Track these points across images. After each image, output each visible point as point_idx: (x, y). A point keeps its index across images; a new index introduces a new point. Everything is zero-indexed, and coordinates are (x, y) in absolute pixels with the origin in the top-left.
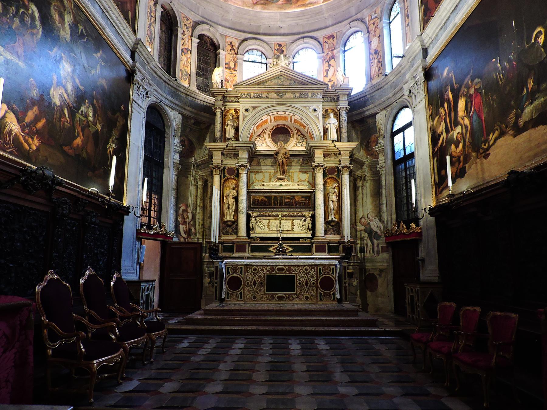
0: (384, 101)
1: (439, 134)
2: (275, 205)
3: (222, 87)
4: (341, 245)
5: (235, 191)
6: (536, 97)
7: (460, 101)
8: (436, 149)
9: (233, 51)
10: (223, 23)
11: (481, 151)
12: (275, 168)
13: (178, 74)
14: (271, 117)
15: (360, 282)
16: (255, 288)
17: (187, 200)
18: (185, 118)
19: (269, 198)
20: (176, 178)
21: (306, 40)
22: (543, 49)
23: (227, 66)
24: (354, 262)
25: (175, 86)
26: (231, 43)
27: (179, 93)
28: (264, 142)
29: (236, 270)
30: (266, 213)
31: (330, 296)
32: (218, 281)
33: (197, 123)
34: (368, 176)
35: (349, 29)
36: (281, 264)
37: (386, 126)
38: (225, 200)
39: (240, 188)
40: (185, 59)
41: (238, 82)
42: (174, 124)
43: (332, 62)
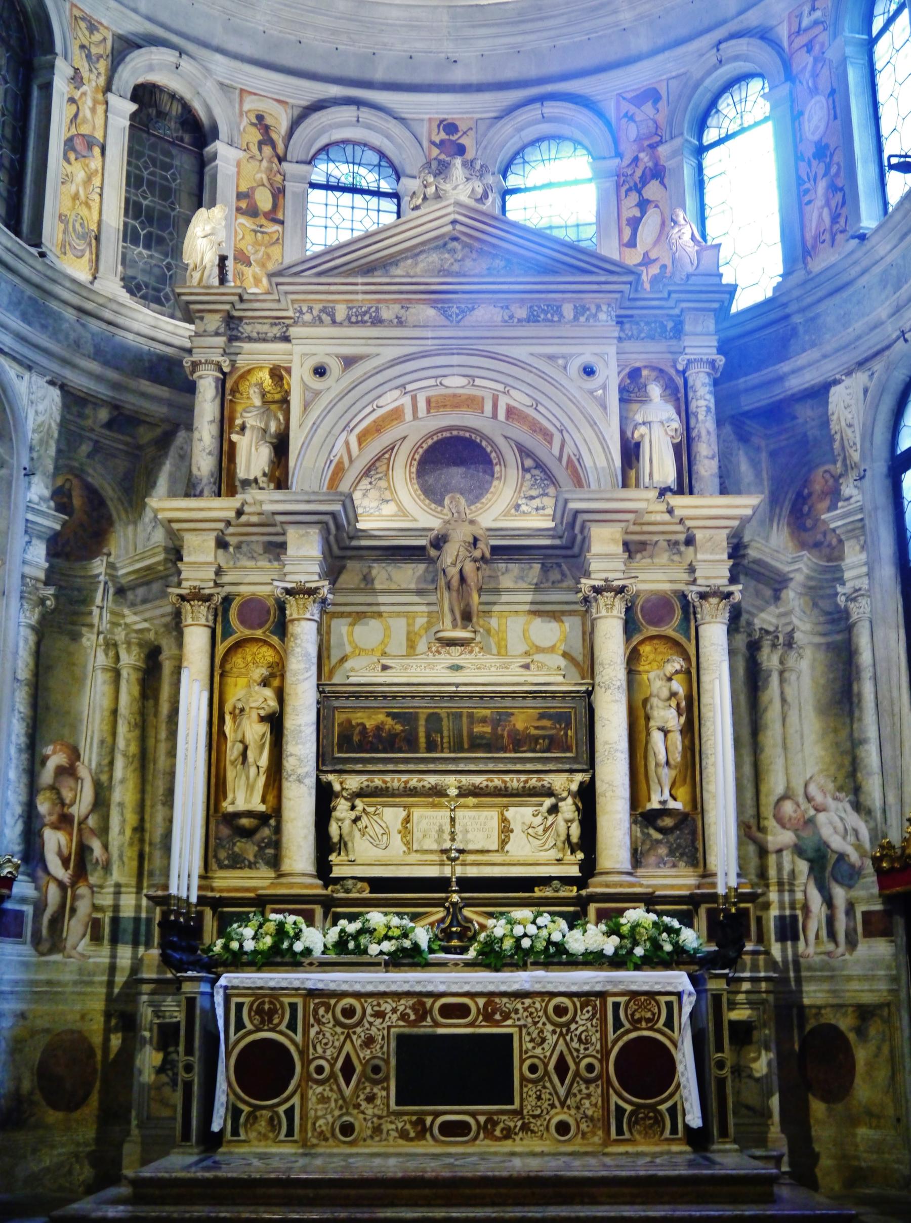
0: (859, 337)
2: (431, 746)
3: (223, 280)
4: (703, 910)
5: (268, 693)
9: (267, 150)
10: (232, 44)
12: (432, 598)
13: (52, 231)
14: (414, 399)
15: (782, 1059)
16: (348, 1092)
17: (74, 727)
18: (74, 401)
19: (407, 719)
20: (32, 638)
21: (552, 108)
23: (243, 205)
24: (752, 980)
25: (36, 279)
26: (260, 118)
27: (54, 305)
28: (387, 495)
29: (272, 1012)
30: (395, 782)
31: (658, 1120)
32: (195, 1059)
33: (123, 420)
34: (805, 627)
35: (715, 68)
36: (455, 989)
37: (868, 435)
38: (228, 728)
39: (290, 679)
40: (80, 176)
41: (288, 261)
42: (30, 424)
43: (652, 190)
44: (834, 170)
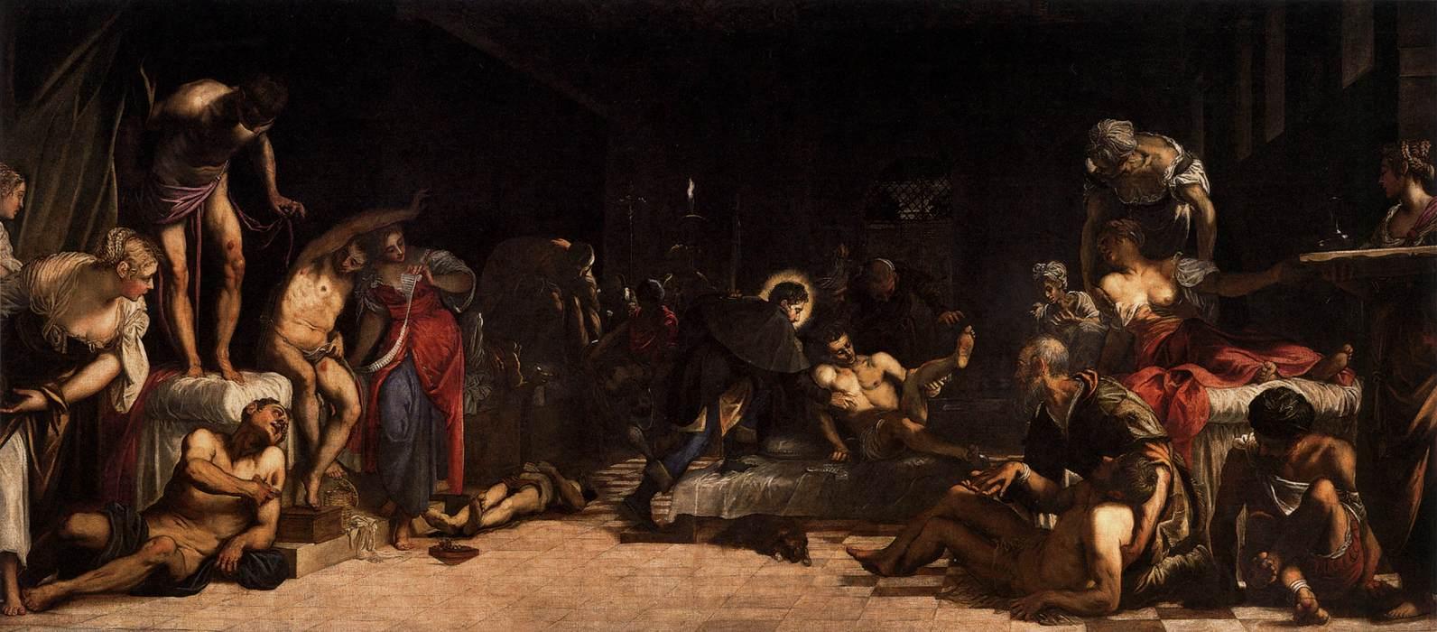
8: (36, 400)
11: (419, 524)
22: (799, 344)
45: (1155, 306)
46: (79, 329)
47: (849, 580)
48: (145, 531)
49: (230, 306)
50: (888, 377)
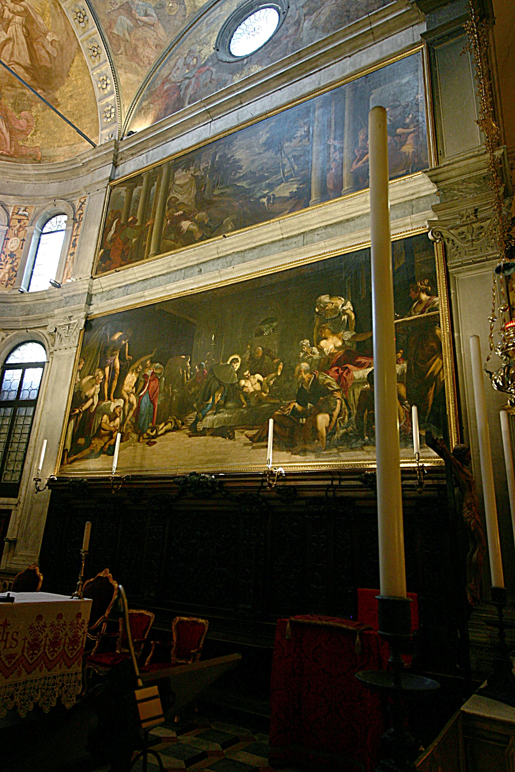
0: (8, 321)
1: (86, 396)
6: (221, 410)
7: (129, 375)
8: (77, 411)
11: (145, 436)
44: (15, 264)
45: (336, 348)
46: (87, 394)
47: (246, 445)
48: (91, 441)
49: (115, 383)
50: (259, 381)
